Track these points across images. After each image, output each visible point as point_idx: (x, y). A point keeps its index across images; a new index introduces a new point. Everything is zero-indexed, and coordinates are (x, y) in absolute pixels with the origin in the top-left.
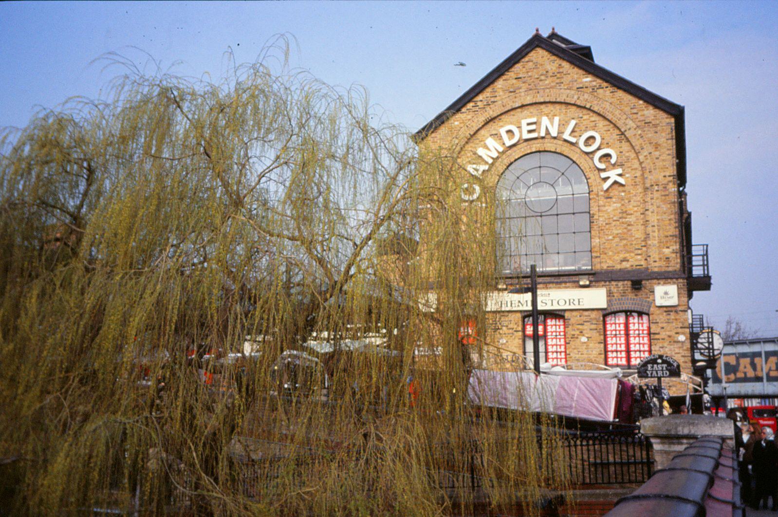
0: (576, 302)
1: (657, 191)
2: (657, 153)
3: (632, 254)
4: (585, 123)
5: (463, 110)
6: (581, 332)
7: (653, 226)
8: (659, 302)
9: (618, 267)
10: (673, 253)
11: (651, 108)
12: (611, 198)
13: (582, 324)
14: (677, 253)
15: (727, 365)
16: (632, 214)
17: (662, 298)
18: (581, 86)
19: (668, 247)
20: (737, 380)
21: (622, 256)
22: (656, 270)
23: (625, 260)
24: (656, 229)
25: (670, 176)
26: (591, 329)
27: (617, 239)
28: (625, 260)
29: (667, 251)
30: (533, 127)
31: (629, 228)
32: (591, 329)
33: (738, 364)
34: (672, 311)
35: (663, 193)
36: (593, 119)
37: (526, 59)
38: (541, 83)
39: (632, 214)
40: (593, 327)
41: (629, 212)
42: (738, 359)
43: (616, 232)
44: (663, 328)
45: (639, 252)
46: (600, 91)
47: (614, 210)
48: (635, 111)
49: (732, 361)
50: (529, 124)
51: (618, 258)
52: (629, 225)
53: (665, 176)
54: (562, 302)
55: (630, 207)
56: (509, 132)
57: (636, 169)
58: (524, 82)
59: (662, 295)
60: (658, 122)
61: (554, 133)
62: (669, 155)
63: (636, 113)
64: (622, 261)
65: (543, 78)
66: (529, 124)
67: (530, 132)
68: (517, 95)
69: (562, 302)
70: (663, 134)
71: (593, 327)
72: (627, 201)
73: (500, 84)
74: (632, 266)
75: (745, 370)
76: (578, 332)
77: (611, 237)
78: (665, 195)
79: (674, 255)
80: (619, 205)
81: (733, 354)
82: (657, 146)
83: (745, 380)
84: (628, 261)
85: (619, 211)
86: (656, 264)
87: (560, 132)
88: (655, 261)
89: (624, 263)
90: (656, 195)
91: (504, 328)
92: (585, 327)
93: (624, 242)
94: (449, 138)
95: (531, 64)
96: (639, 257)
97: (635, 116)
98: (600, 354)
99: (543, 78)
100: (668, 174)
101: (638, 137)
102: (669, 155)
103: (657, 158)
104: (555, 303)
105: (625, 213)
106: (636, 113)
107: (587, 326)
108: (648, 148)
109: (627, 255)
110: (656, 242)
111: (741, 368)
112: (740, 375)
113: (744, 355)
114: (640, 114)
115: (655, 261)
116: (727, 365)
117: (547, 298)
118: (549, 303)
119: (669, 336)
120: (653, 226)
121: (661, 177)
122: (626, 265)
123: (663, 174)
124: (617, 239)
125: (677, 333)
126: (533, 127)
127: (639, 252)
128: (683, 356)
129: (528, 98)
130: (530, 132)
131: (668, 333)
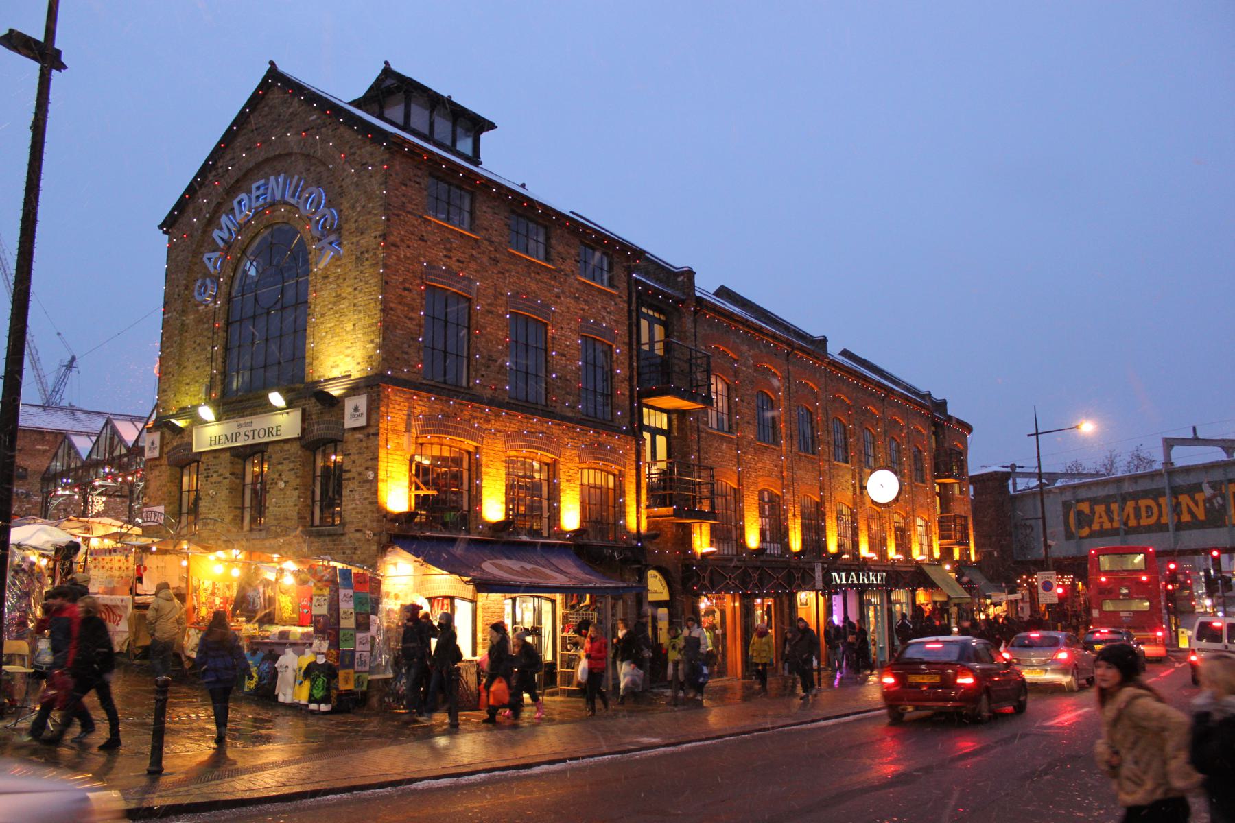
8: (349, 423)
17: (352, 416)
20: (1093, 534)
33: (1093, 511)
40: (291, 465)
41: (344, 295)
46: (324, 130)
49: (1085, 507)
54: (262, 434)
61: (278, 197)
66: (258, 188)
71: (291, 465)
76: (276, 476)
83: (1102, 533)
87: (283, 195)
100: (378, 233)
107: (288, 466)
111: (1097, 516)
112: (1096, 527)
116: (1079, 513)
118: (251, 434)
119: (360, 474)
125: (367, 469)
131: (360, 469)
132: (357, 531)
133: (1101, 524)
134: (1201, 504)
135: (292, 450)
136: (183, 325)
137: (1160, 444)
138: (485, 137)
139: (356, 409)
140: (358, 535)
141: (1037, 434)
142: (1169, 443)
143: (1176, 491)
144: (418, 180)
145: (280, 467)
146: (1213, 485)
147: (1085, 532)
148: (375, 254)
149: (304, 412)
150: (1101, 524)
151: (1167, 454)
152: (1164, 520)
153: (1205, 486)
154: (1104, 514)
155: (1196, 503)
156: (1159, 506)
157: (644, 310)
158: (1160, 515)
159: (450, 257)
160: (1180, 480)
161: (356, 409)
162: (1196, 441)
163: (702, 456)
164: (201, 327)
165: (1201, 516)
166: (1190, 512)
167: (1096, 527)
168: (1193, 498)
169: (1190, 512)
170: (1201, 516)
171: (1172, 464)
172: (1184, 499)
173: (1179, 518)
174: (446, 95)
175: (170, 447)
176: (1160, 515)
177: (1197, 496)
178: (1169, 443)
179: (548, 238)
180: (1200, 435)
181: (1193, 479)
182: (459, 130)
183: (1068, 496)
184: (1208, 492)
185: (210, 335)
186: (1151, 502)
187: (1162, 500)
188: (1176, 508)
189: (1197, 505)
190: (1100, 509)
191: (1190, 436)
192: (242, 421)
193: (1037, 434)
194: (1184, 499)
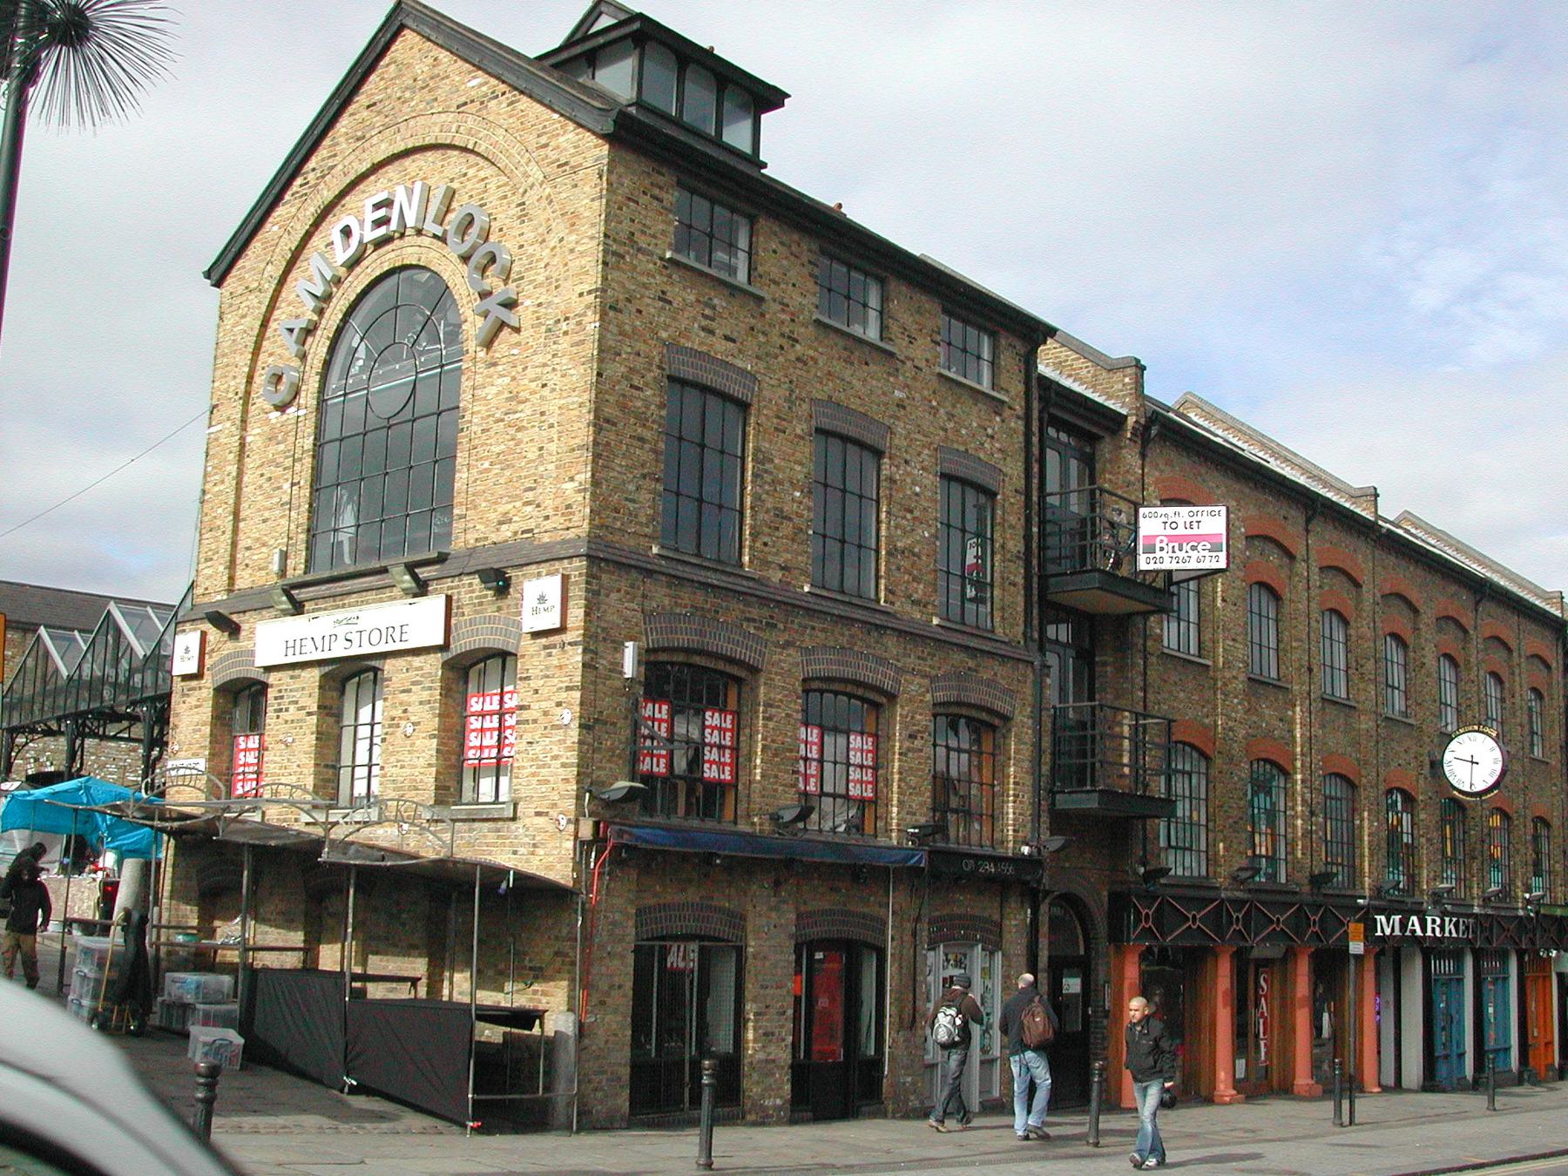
0: (397, 636)
1: (566, 333)
2: (573, 237)
3: (518, 504)
4: (469, 185)
5: (287, 197)
6: (405, 711)
7: (552, 426)
9: (494, 537)
10: (579, 491)
11: (571, 126)
12: (495, 364)
13: (409, 691)
14: (585, 490)
16: (527, 400)
17: (535, 611)
18: (463, 99)
19: (572, 479)
21: (502, 509)
22: (546, 539)
23: (505, 520)
24: (554, 433)
25: (590, 292)
26: (421, 703)
27: (496, 469)
28: (505, 520)
29: (570, 486)
30: (382, 212)
31: (519, 435)
32: (421, 703)
34: (554, 647)
35: (577, 338)
36: (482, 174)
37: (386, 60)
38: (406, 109)
39: (527, 400)
40: (425, 695)
43: (496, 449)
44: (536, 692)
45: (530, 495)
47: (499, 393)
48: (543, 140)
50: (377, 206)
51: (493, 516)
52: (519, 430)
53: (581, 295)
55: (527, 385)
56: (347, 232)
57: (541, 285)
58: (379, 112)
59: (535, 603)
60: (579, 159)
61: (411, 221)
62: (592, 238)
63: (546, 146)
64: (501, 523)
65: (408, 94)
66: (377, 206)
67: (378, 223)
68: (367, 145)
69: (375, 637)
70: (587, 189)
72: (520, 369)
73: (344, 124)
74: (515, 533)
77: (486, 465)
78: (577, 344)
79: (579, 497)
80: (507, 380)
82: (573, 220)
84: (510, 521)
85: (507, 395)
86: (548, 525)
88: (547, 518)
89: (504, 527)
90: (565, 343)
91: (292, 708)
92: (413, 698)
93: (507, 473)
94: (262, 265)
95: (393, 67)
96: (529, 509)
97: (543, 152)
98: (430, 765)
99: (408, 94)
100: (586, 287)
101: (544, 203)
102: (592, 238)
103: (572, 251)
104: (365, 636)
105: (514, 397)
106: (546, 146)
108: (560, 228)
109: (510, 506)
110: (551, 467)
114: (553, 144)
115: (547, 518)
117: (354, 628)
119: (546, 713)
120: (552, 426)
121: (575, 297)
122: (506, 532)
123: (578, 289)
124: (496, 469)
125: (559, 704)
126: (382, 212)
127: (530, 495)
128: (564, 765)
129: (383, 146)
130: (378, 223)
131: (544, 705)
132: (538, 814)
135: (427, 669)
136: (242, 445)
138: (767, 119)
139: (542, 599)
140: (541, 820)
144: (656, 192)
145: (404, 697)
148: (579, 323)
149: (449, 599)
157: (1052, 432)
159: (712, 332)
161: (542, 599)
163: (1151, 697)
164: (272, 449)
174: (706, 46)
175: (216, 657)
179: (884, 300)
182: (727, 105)
185: (288, 462)
192: (340, 614)
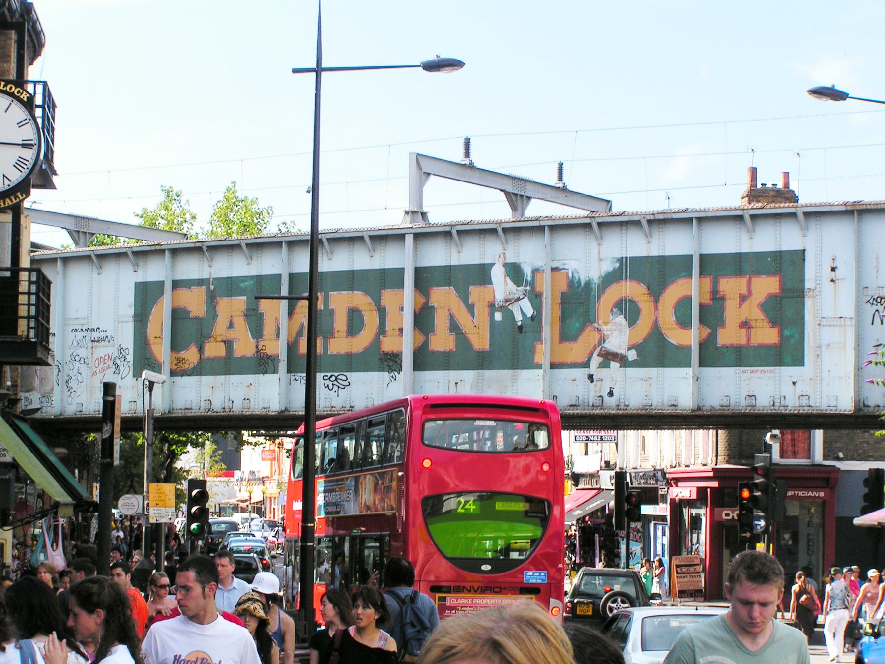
15: (178, 315)
42: (212, 299)
49: (195, 303)
75: (231, 335)
81: (200, 282)
83: (229, 365)
111: (220, 328)
112: (214, 349)
113: (231, 286)
133: (228, 344)
134: (481, 310)
137: (404, 169)
141: (318, 70)
142: (424, 167)
143: (425, 278)
146: (514, 272)
147: (191, 355)
150: (228, 344)
151: (418, 194)
152: (388, 345)
153: (498, 274)
154: (241, 323)
155: (471, 309)
156: (382, 312)
158: (382, 330)
160: (437, 255)
162: (467, 171)
165: (480, 341)
166: (454, 327)
167: (214, 349)
168: (464, 296)
169: (454, 327)
170: (480, 341)
171: (424, 215)
172: (443, 297)
173: (426, 343)
176: (382, 330)
177: (475, 292)
178: (424, 167)
180: (479, 159)
181: (470, 254)
183: (155, 271)
184: (501, 286)
186: (360, 299)
187: (388, 297)
188: (423, 319)
189: (471, 309)
190: (233, 307)
191: (458, 157)
193: (318, 70)
194: (443, 297)
